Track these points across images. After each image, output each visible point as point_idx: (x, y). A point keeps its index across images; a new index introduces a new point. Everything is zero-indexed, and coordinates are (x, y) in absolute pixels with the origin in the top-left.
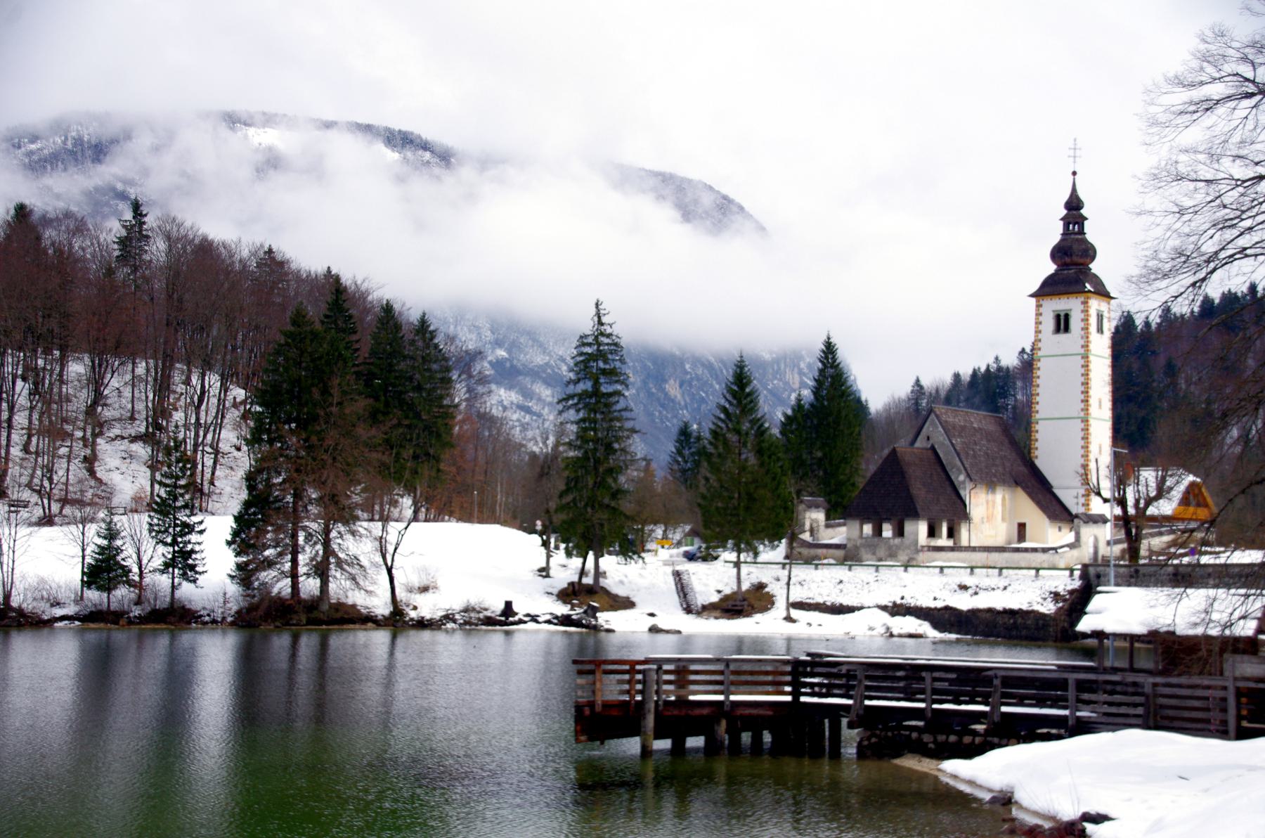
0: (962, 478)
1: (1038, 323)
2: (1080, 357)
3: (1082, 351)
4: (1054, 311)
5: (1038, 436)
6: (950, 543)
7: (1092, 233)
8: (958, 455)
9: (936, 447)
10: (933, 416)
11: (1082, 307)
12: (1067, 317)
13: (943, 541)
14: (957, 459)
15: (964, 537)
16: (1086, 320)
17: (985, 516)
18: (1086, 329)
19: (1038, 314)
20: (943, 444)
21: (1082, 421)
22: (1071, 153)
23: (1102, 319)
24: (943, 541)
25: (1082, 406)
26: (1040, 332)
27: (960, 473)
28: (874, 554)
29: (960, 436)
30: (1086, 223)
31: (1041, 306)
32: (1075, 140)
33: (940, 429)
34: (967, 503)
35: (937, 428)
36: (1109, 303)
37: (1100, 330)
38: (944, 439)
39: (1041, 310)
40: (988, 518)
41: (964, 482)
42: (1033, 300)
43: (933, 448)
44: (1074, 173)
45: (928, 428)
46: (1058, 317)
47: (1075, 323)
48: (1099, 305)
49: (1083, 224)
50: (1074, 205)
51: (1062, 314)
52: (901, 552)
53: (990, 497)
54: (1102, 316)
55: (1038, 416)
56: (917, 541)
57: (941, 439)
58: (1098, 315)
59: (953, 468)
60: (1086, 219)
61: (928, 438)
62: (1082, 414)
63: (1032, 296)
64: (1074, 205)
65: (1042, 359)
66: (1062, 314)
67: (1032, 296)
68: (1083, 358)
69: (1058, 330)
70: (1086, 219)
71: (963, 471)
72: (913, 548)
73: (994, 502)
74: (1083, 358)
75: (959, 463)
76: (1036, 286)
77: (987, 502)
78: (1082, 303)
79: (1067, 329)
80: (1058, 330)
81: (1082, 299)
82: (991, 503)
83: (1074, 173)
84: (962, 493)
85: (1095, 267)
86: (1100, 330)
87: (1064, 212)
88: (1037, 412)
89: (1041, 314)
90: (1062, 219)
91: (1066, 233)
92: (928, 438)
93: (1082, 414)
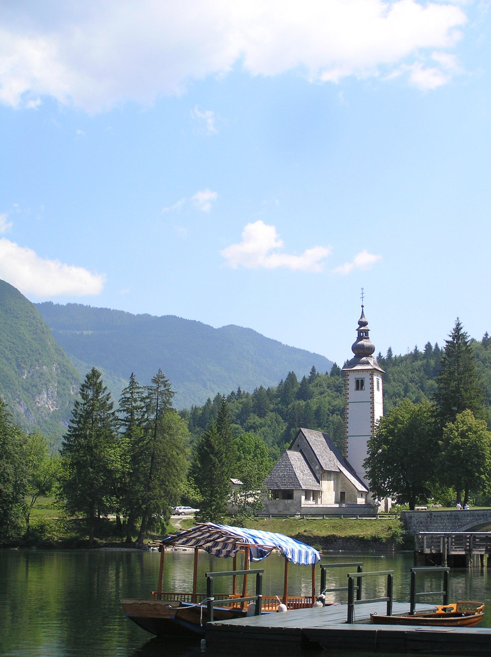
0: (317, 467)
2: (370, 403)
4: (355, 378)
9: (303, 451)
16: (372, 384)
18: (372, 388)
28: (276, 509)
35: (303, 440)
46: (357, 382)
55: (348, 434)
59: (312, 462)
61: (298, 446)
62: (371, 434)
69: (357, 388)
71: (318, 464)
74: (371, 404)
78: (370, 374)
80: (357, 388)
81: (370, 373)
83: (362, 306)
91: (360, 338)
92: (298, 446)
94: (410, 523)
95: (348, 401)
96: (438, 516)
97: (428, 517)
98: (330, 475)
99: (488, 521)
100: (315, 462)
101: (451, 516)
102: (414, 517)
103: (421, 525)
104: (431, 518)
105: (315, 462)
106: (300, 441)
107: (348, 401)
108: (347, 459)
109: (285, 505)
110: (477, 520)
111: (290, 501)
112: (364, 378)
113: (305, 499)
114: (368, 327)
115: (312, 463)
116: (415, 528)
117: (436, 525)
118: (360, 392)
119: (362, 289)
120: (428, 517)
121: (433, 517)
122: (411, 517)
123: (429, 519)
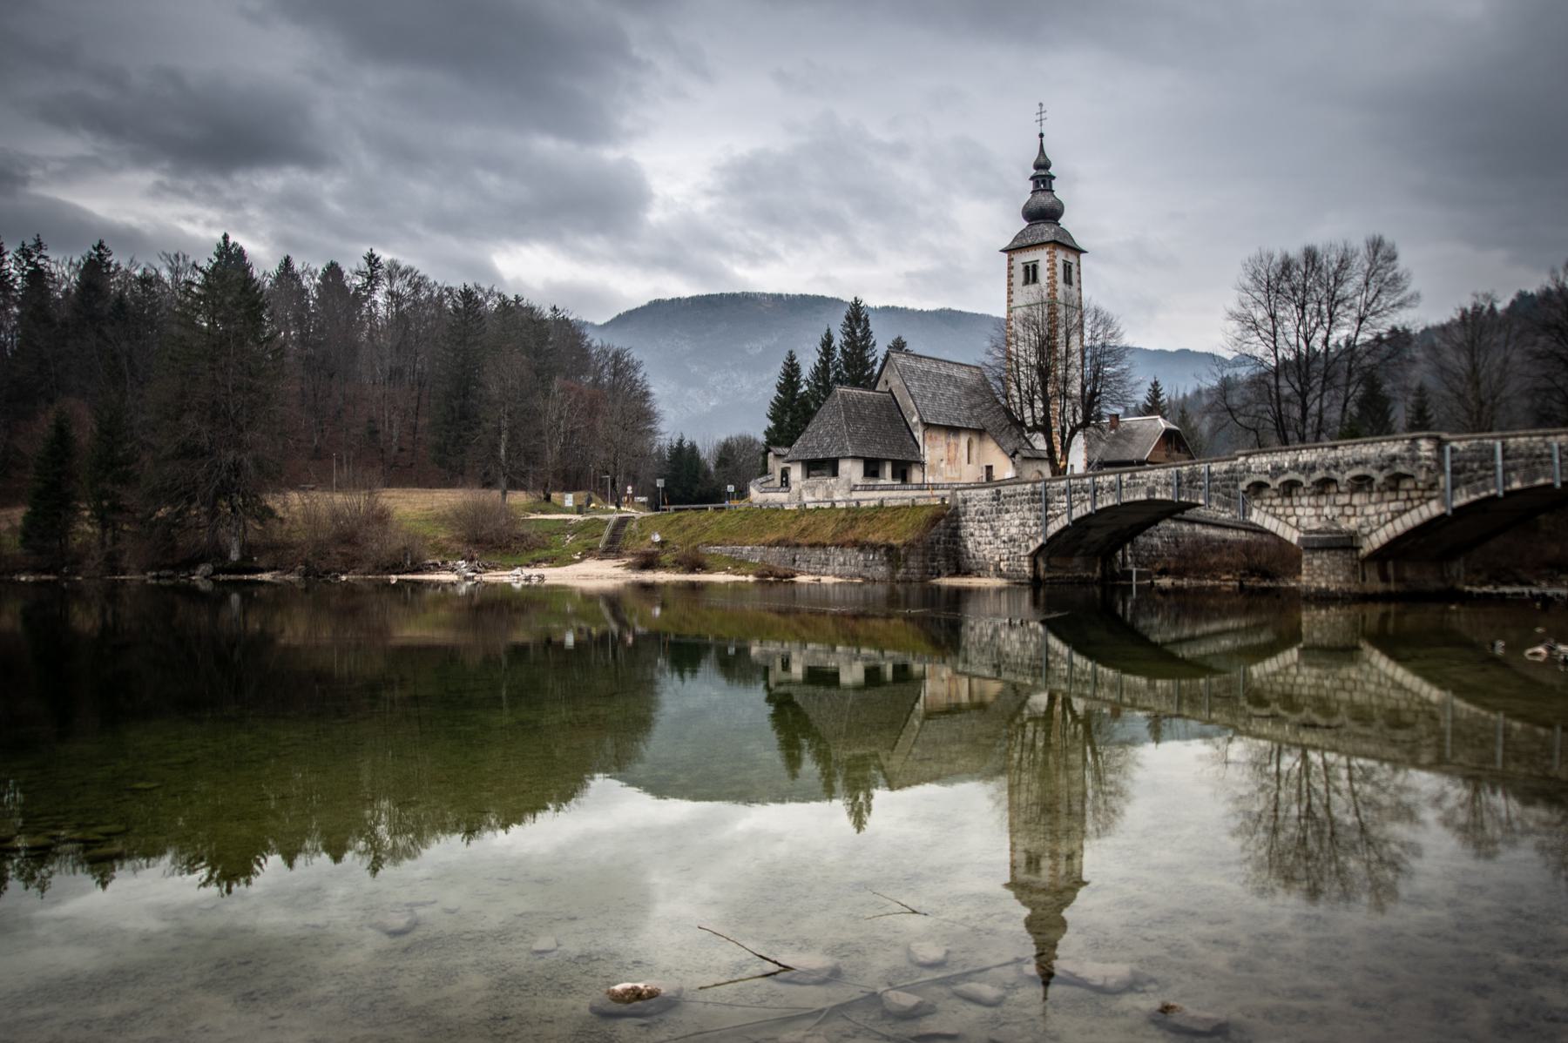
0: (915, 419)
1: (1010, 276)
7: (1060, 190)
8: (912, 396)
10: (890, 360)
11: (1047, 257)
12: (1035, 267)
13: (887, 477)
15: (916, 476)
17: (945, 457)
19: (1010, 268)
20: (900, 388)
22: (1038, 117)
23: (1070, 271)
24: (887, 477)
26: (1012, 284)
27: (913, 414)
28: (814, 495)
29: (919, 379)
30: (1053, 182)
31: (1012, 259)
32: (1041, 105)
33: (897, 372)
34: (921, 443)
36: (1078, 257)
37: (1068, 280)
39: (1013, 263)
41: (916, 424)
42: (1006, 256)
43: (890, 391)
44: (1041, 135)
46: (1027, 268)
47: (1043, 275)
48: (1067, 256)
49: (1050, 182)
50: (1042, 164)
51: (1030, 265)
52: (836, 492)
53: (952, 440)
54: (1070, 267)
56: (849, 480)
57: (898, 382)
58: (1065, 265)
60: (1054, 178)
63: (1003, 251)
64: (1042, 164)
66: (1030, 265)
67: (1003, 251)
69: (1026, 282)
70: (1054, 178)
72: (846, 487)
73: (957, 446)
76: (1006, 242)
77: (948, 445)
78: (1048, 253)
79: (1035, 280)
80: (1026, 282)
82: (953, 447)
83: (1041, 135)
84: (916, 434)
85: (1064, 221)
86: (1068, 280)
87: (1033, 172)
89: (1012, 268)
90: (1032, 178)
94: (965, 514)
95: (1012, 305)
96: (1010, 496)
97: (994, 499)
99: (1105, 504)
101: (1033, 493)
102: (971, 500)
103: (982, 518)
104: (999, 500)
107: (1012, 305)
109: (827, 488)
110: (1082, 500)
111: (833, 480)
114: (1052, 171)
116: (971, 524)
117: (1007, 517)
118: (1032, 288)
119: (1041, 105)
120: (994, 499)
121: (1002, 499)
122: (965, 502)
123: (995, 503)
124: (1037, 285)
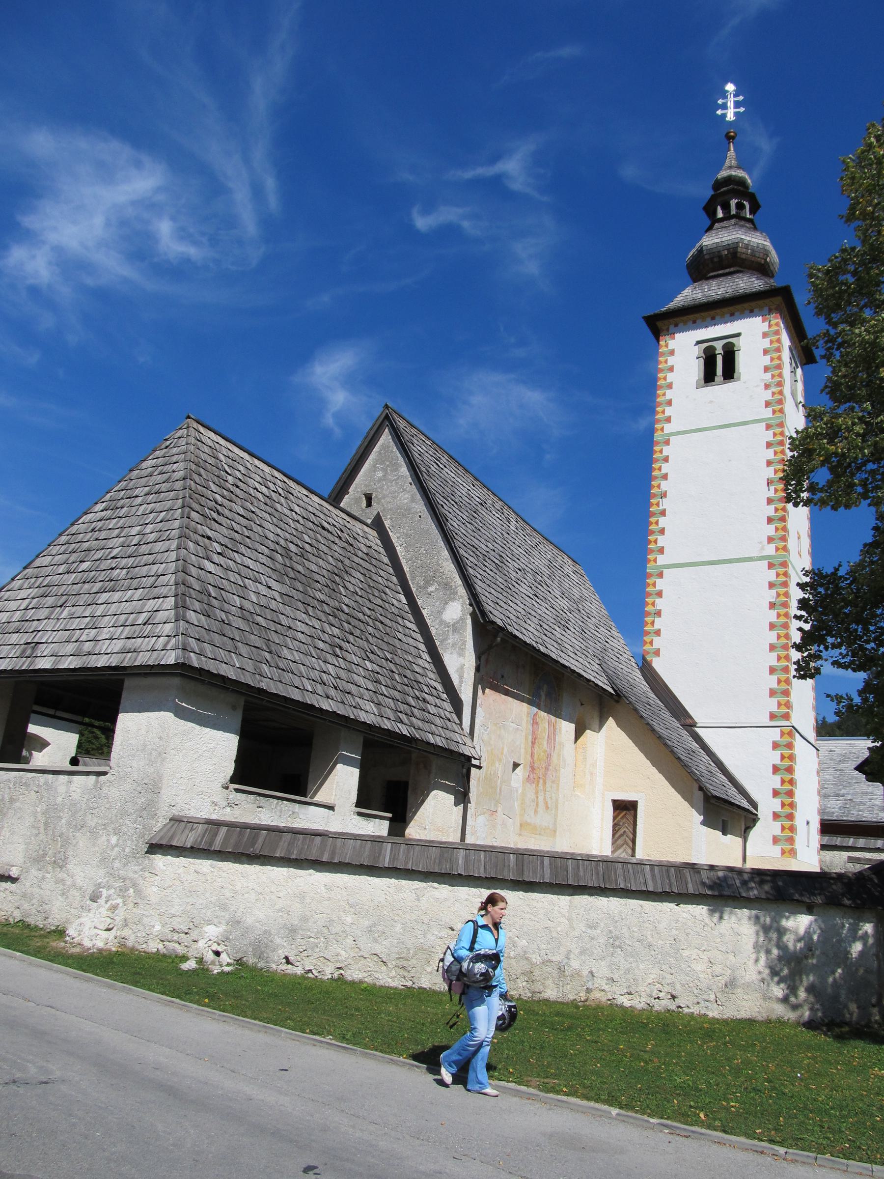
2: (764, 424)
3: (768, 413)
4: (698, 343)
5: (660, 603)
6: (379, 827)
9: (387, 523)
14: (446, 553)
21: (771, 566)
25: (770, 530)
34: (466, 695)
35: (396, 468)
38: (413, 500)
40: (533, 769)
41: (456, 627)
45: (374, 468)
51: (719, 346)
59: (428, 583)
62: (770, 550)
65: (672, 439)
66: (719, 346)
68: (768, 427)
71: (462, 591)
72: (129, 825)
74: (768, 427)
75: (449, 567)
77: (535, 723)
88: (661, 551)
93: (770, 550)
98: (548, 695)
100: (447, 586)
105: (447, 586)
106: (380, 474)
108: (657, 664)
112: (738, 335)
113: (233, 780)
115: (425, 588)
118: (720, 390)
124: (731, 386)
